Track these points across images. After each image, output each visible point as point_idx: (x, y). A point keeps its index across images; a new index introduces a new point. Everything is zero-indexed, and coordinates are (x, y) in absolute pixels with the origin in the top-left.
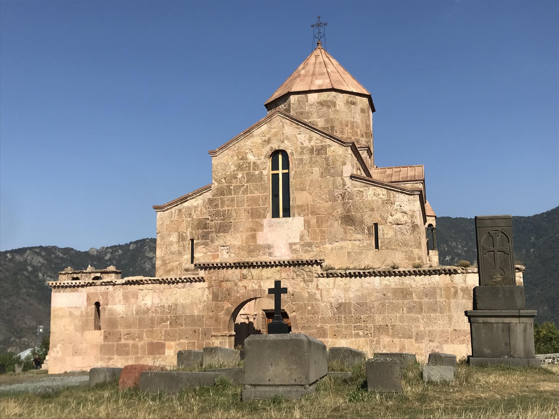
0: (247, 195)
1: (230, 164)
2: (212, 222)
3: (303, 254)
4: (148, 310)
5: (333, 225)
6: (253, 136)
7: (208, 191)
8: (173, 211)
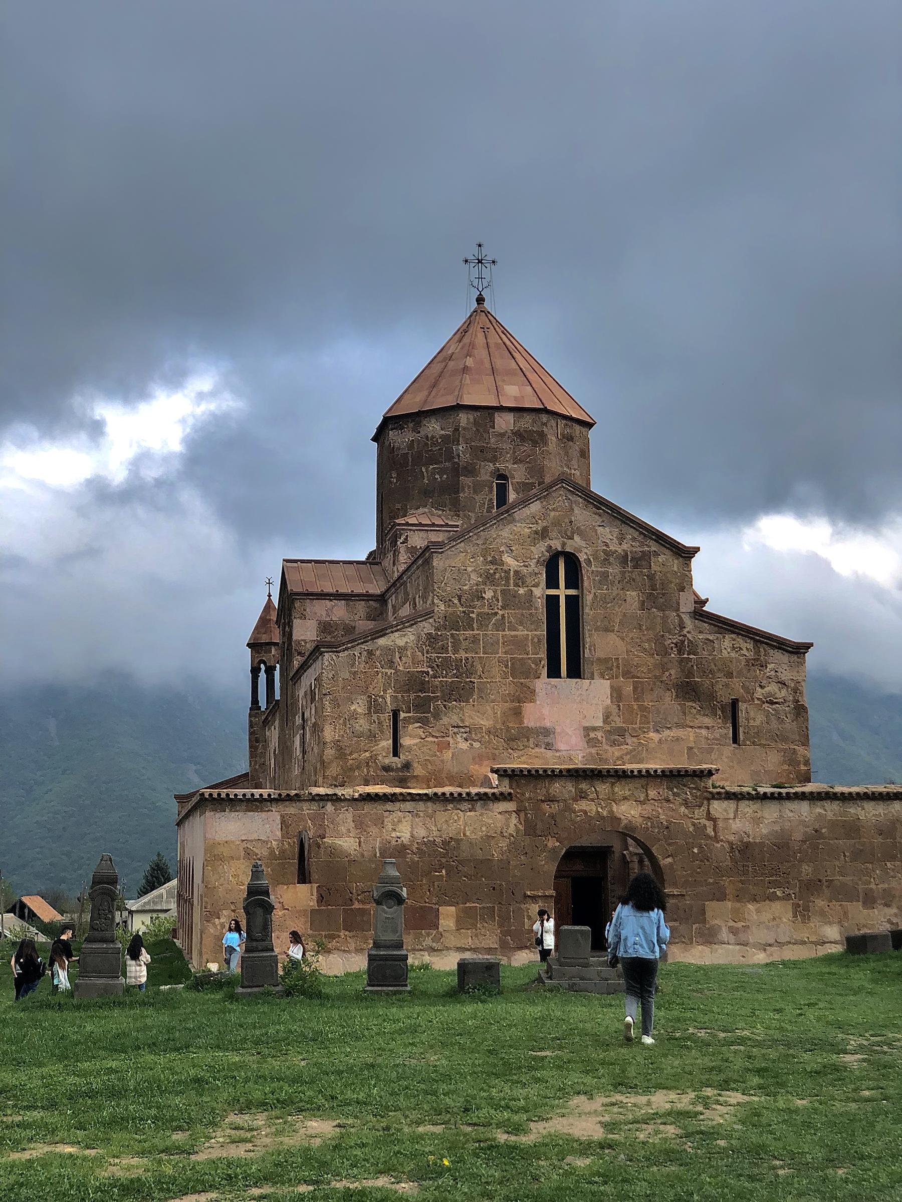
0: (504, 633)
1: (469, 569)
2: (436, 680)
3: (608, 747)
4: (404, 847)
5: (663, 697)
6: (514, 520)
7: (426, 619)
8: (356, 653)
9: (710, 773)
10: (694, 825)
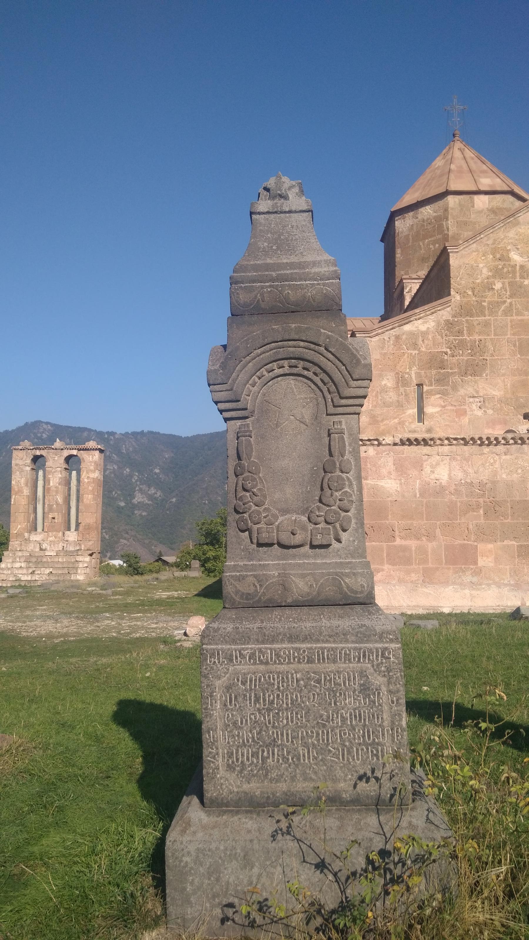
0: (512, 318)
1: (481, 265)
2: (454, 358)
8: (385, 338)
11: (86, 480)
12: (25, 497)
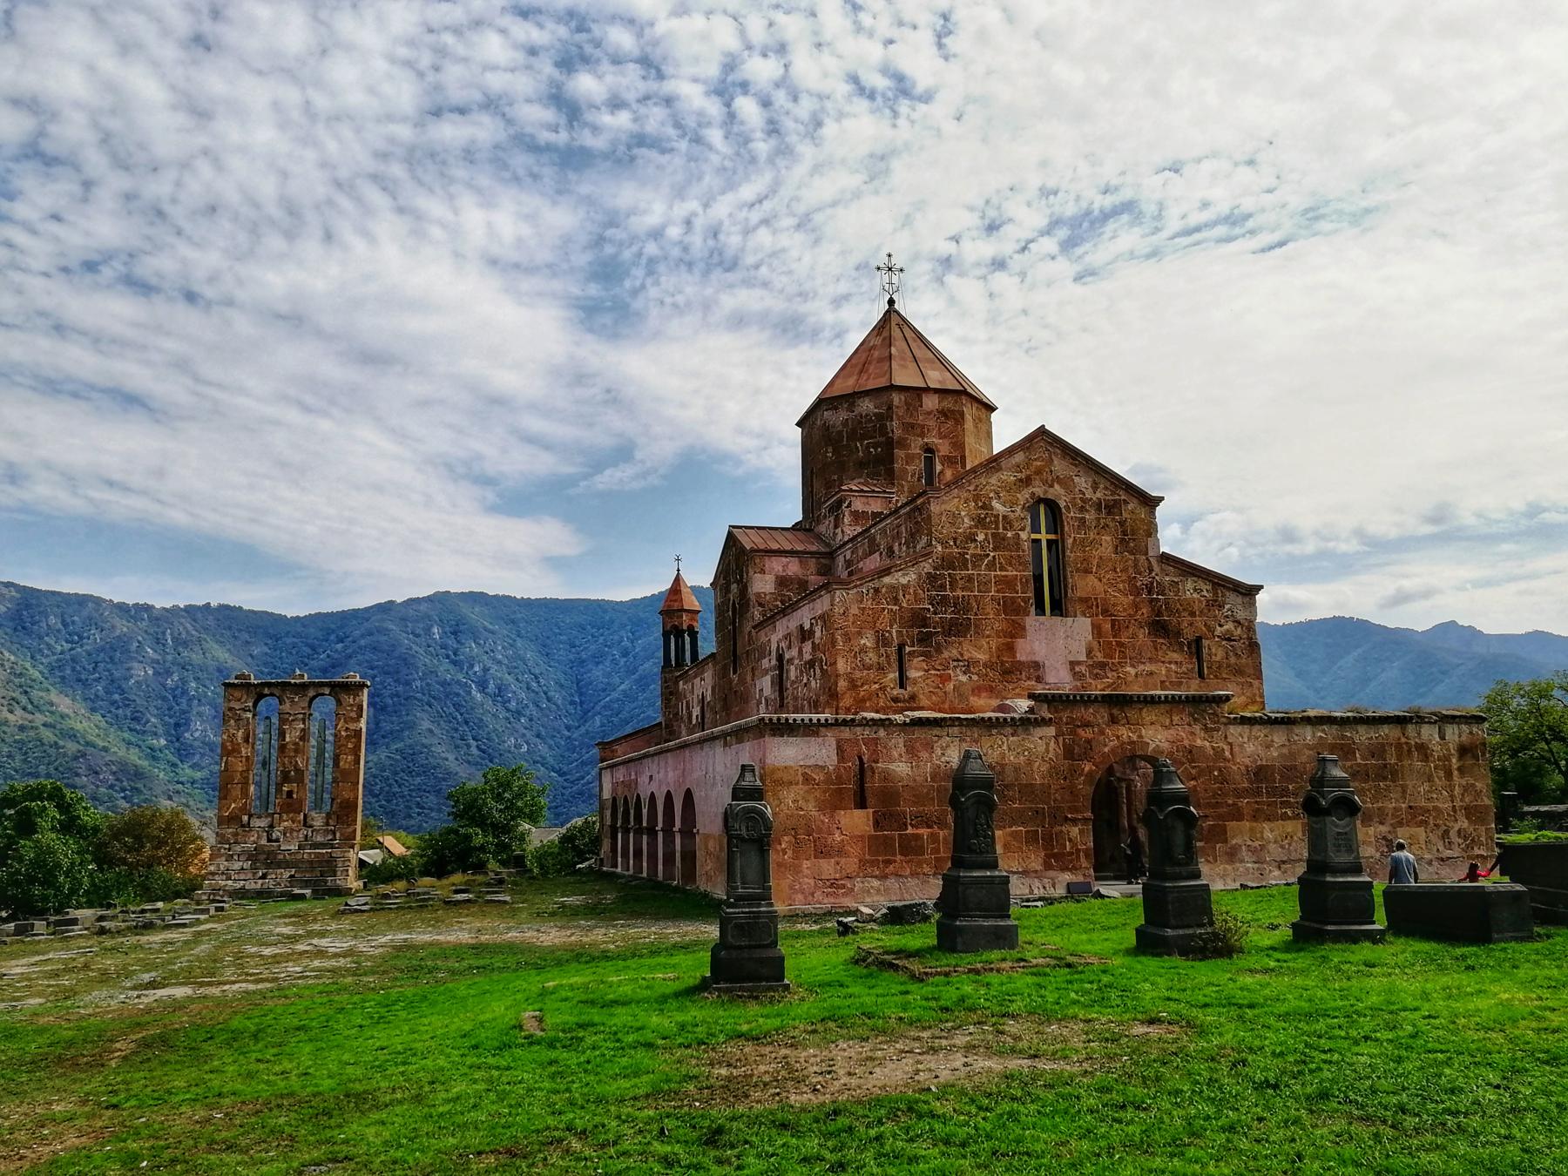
1: (963, 513)
3: (1091, 681)
6: (1001, 469)
9: (1228, 698)
10: (1213, 748)
11: (343, 733)
12: (244, 760)
